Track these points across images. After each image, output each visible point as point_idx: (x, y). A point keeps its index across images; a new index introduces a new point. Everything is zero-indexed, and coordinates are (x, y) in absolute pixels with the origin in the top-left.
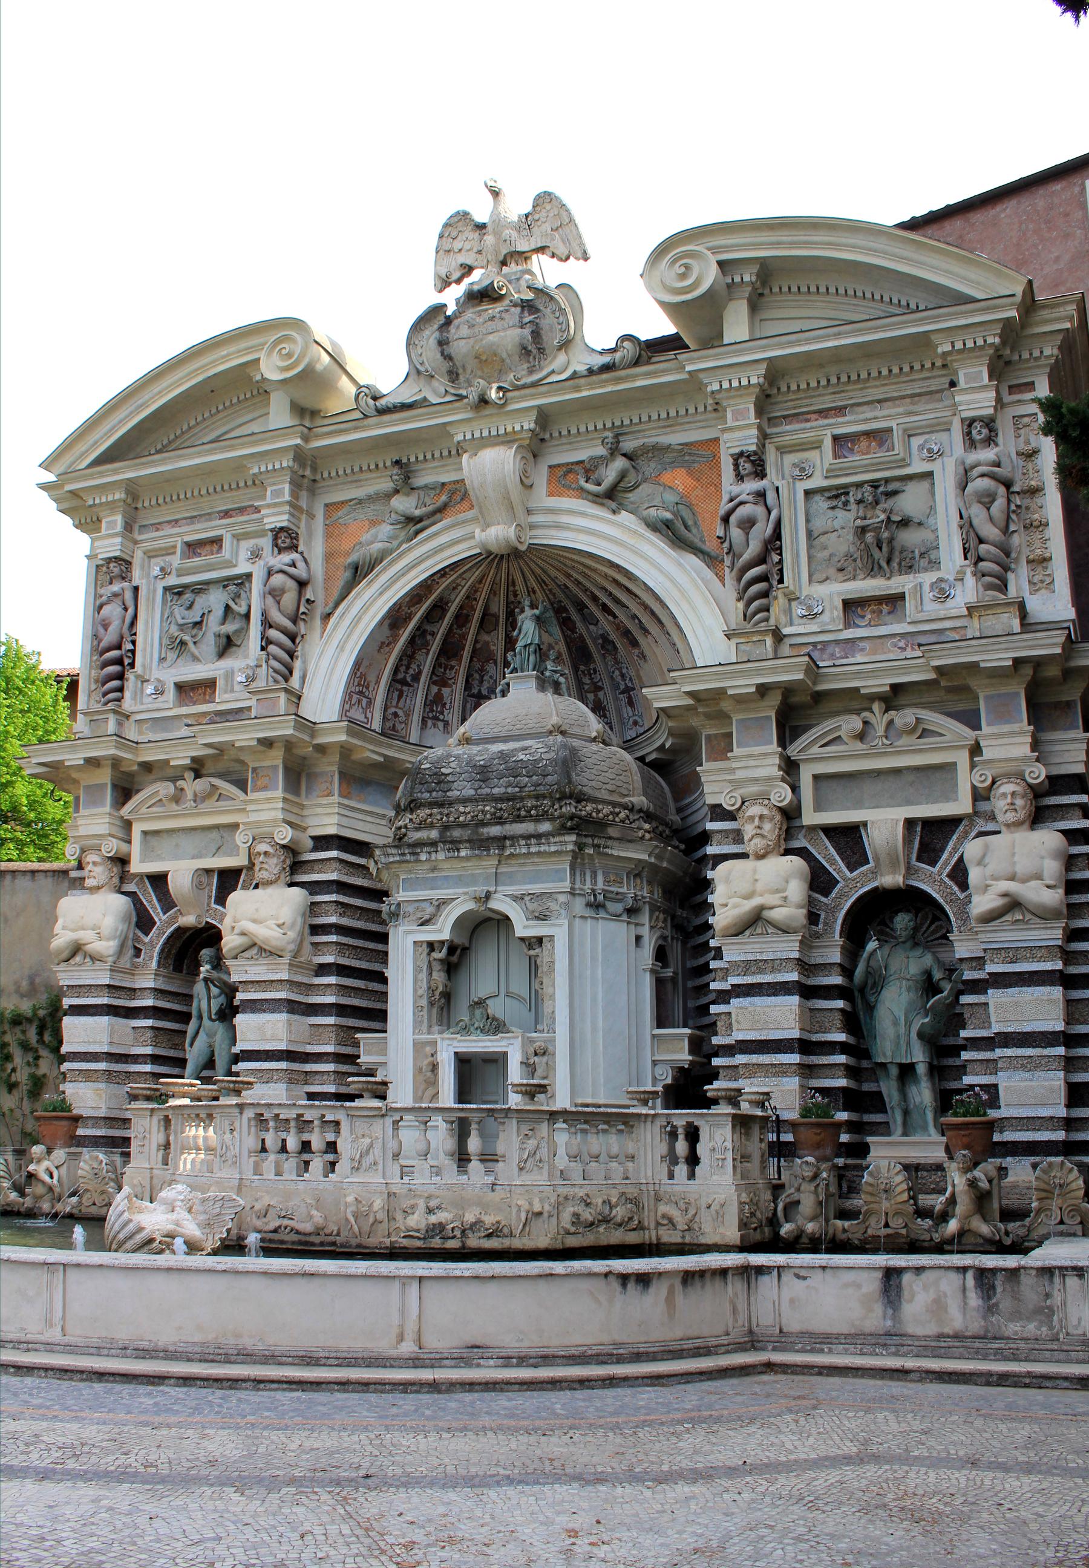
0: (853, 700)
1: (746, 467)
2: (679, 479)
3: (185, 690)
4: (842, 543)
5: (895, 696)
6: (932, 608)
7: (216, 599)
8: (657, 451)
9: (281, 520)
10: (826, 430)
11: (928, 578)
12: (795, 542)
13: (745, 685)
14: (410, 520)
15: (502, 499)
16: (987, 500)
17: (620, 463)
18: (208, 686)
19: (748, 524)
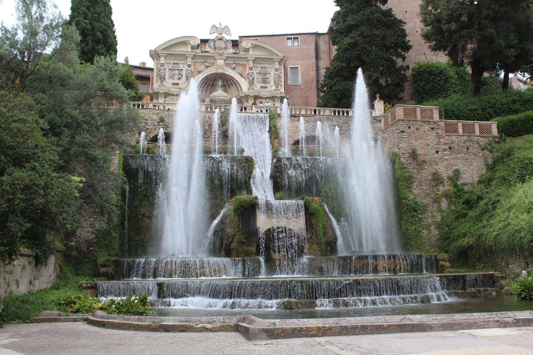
0: (262, 98)
2: (241, 68)
3: (173, 84)
4: (260, 79)
5: (267, 98)
6: (270, 89)
7: (177, 72)
8: (239, 64)
9: (189, 63)
10: (260, 66)
11: (270, 85)
12: (255, 79)
13: (252, 95)
14: (207, 66)
15: (220, 66)
16: (277, 78)
19: (251, 76)
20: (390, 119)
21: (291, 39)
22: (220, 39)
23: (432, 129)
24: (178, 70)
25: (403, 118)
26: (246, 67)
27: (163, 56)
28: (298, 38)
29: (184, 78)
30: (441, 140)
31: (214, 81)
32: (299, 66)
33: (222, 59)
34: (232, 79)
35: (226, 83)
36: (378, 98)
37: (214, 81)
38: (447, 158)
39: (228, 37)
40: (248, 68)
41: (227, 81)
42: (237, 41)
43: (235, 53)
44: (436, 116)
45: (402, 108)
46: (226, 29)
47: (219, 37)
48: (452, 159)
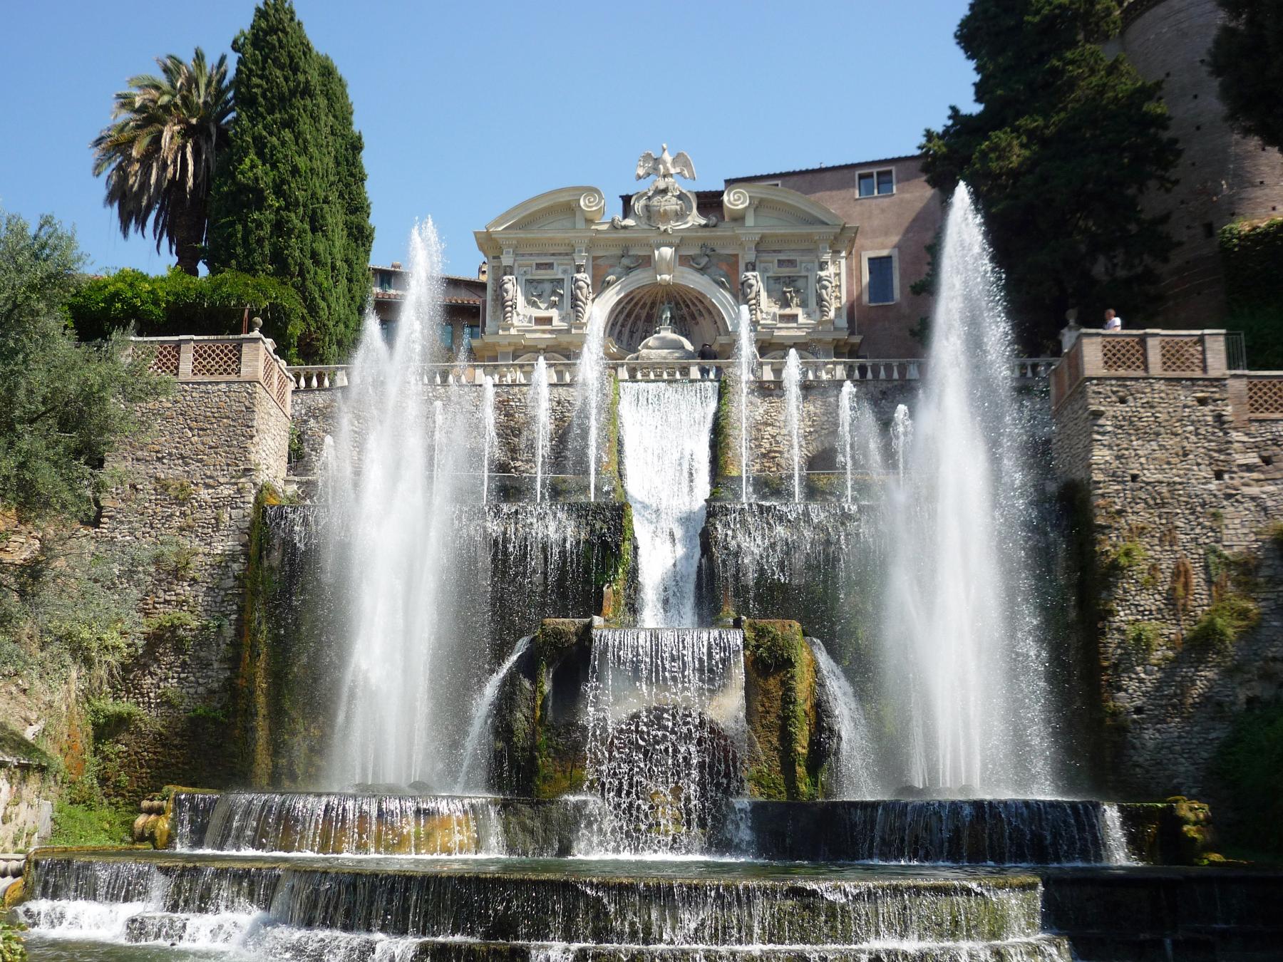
1: (750, 267)
7: (548, 287)
17: (706, 259)
18: (549, 320)
20: (1067, 382)
21: (871, 175)
22: (664, 191)
23: (1202, 402)
24: (552, 281)
26: (737, 262)
27: (509, 246)
28: (890, 172)
29: (567, 301)
30: (1235, 435)
31: (651, 308)
33: (670, 245)
35: (685, 310)
36: (1072, 322)
37: (651, 308)
38: (1254, 490)
40: (742, 266)
41: (687, 306)
43: (706, 226)
44: (1217, 362)
45: (1100, 339)
48: (1272, 495)
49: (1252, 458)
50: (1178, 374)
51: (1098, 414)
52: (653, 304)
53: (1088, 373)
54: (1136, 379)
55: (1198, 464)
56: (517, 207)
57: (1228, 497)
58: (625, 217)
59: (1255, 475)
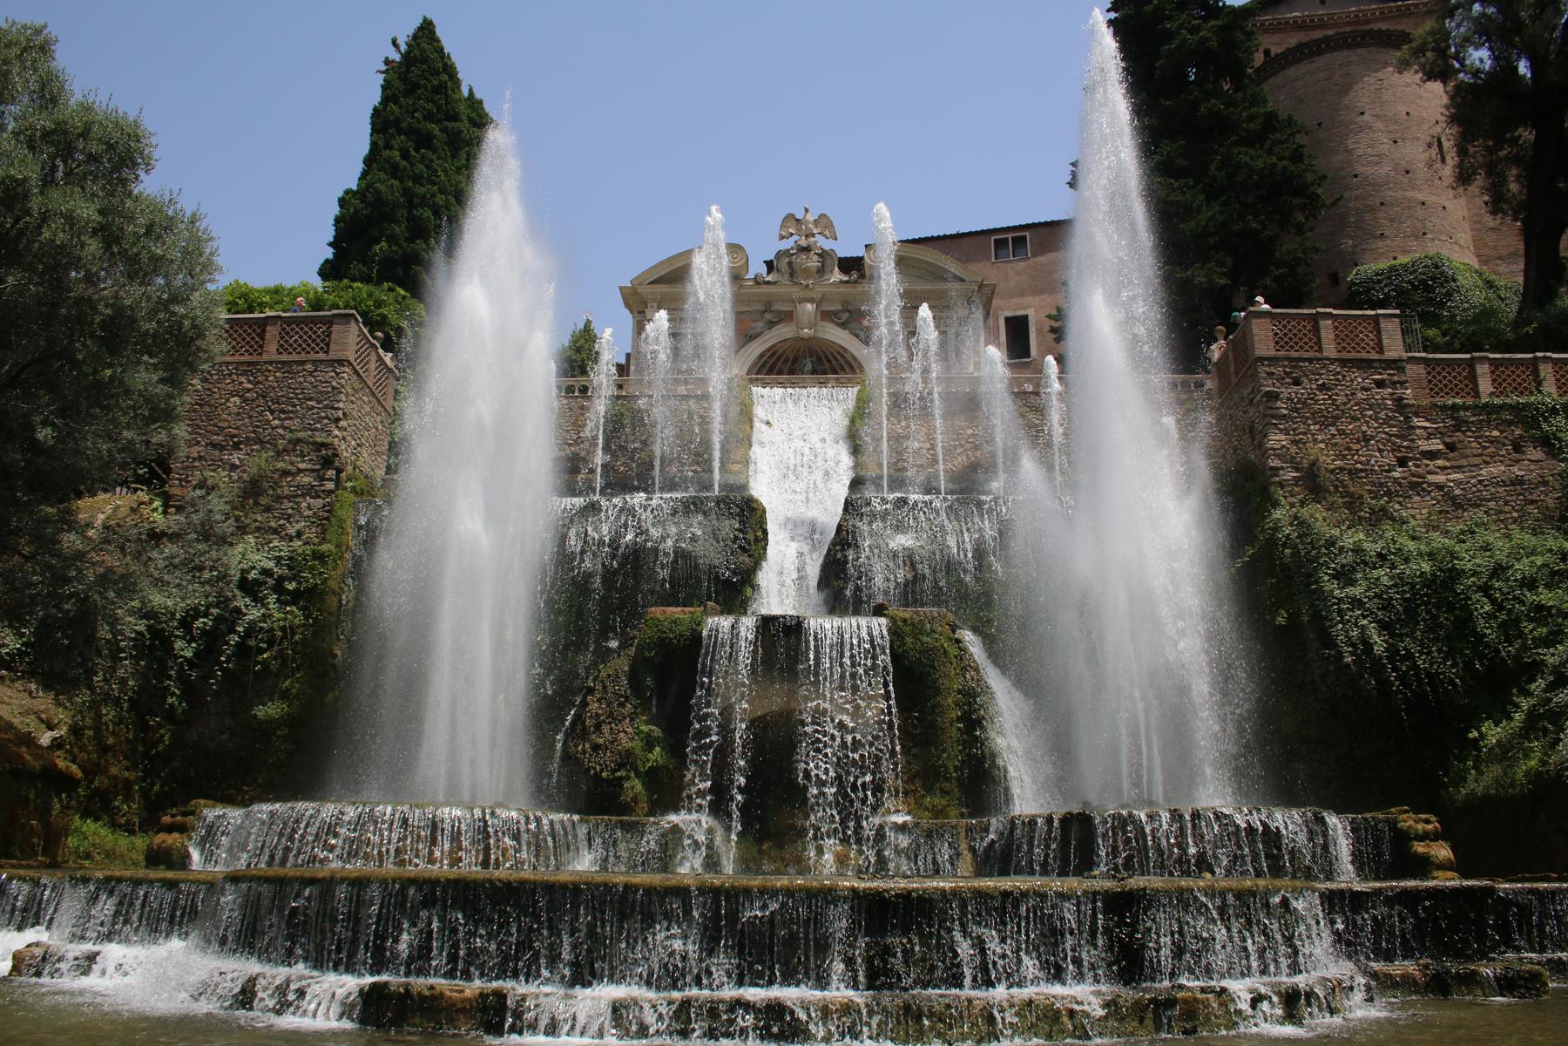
22: (807, 249)
25: (1272, 353)
30: (1416, 422)
32: (1030, 312)
33: (811, 301)
34: (842, 351)
38: (1440, 478)
39: (826, 244)
42: (862, 259)
46: (824, 222)
47: (803, 242)
48: (1458, 483)
49: (1436, 445)
50: (1353, 355)
51: (1274, 396)
52: (796, 359)
53: (1258, 353)
54: (1310, 360)
55: (1380, 451)
56: (662, 263)
57: (1413, 486)
58: (769, 272)
59: (1440, 462)
